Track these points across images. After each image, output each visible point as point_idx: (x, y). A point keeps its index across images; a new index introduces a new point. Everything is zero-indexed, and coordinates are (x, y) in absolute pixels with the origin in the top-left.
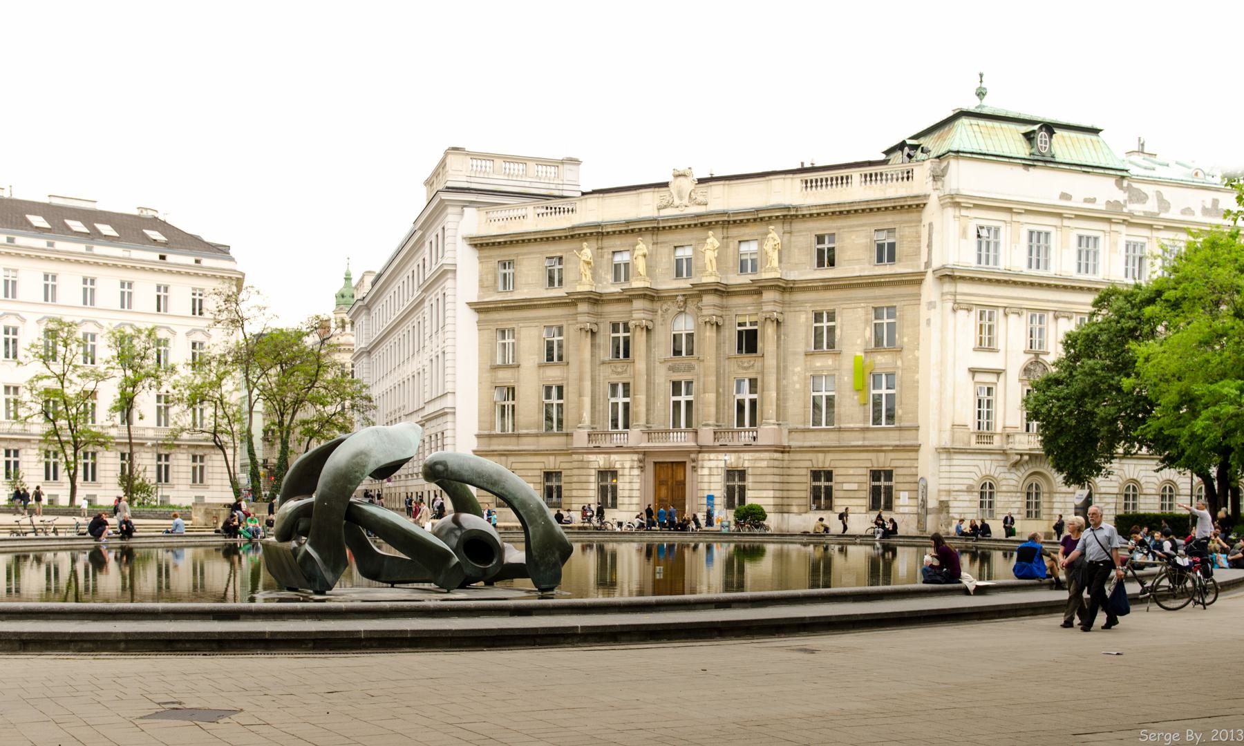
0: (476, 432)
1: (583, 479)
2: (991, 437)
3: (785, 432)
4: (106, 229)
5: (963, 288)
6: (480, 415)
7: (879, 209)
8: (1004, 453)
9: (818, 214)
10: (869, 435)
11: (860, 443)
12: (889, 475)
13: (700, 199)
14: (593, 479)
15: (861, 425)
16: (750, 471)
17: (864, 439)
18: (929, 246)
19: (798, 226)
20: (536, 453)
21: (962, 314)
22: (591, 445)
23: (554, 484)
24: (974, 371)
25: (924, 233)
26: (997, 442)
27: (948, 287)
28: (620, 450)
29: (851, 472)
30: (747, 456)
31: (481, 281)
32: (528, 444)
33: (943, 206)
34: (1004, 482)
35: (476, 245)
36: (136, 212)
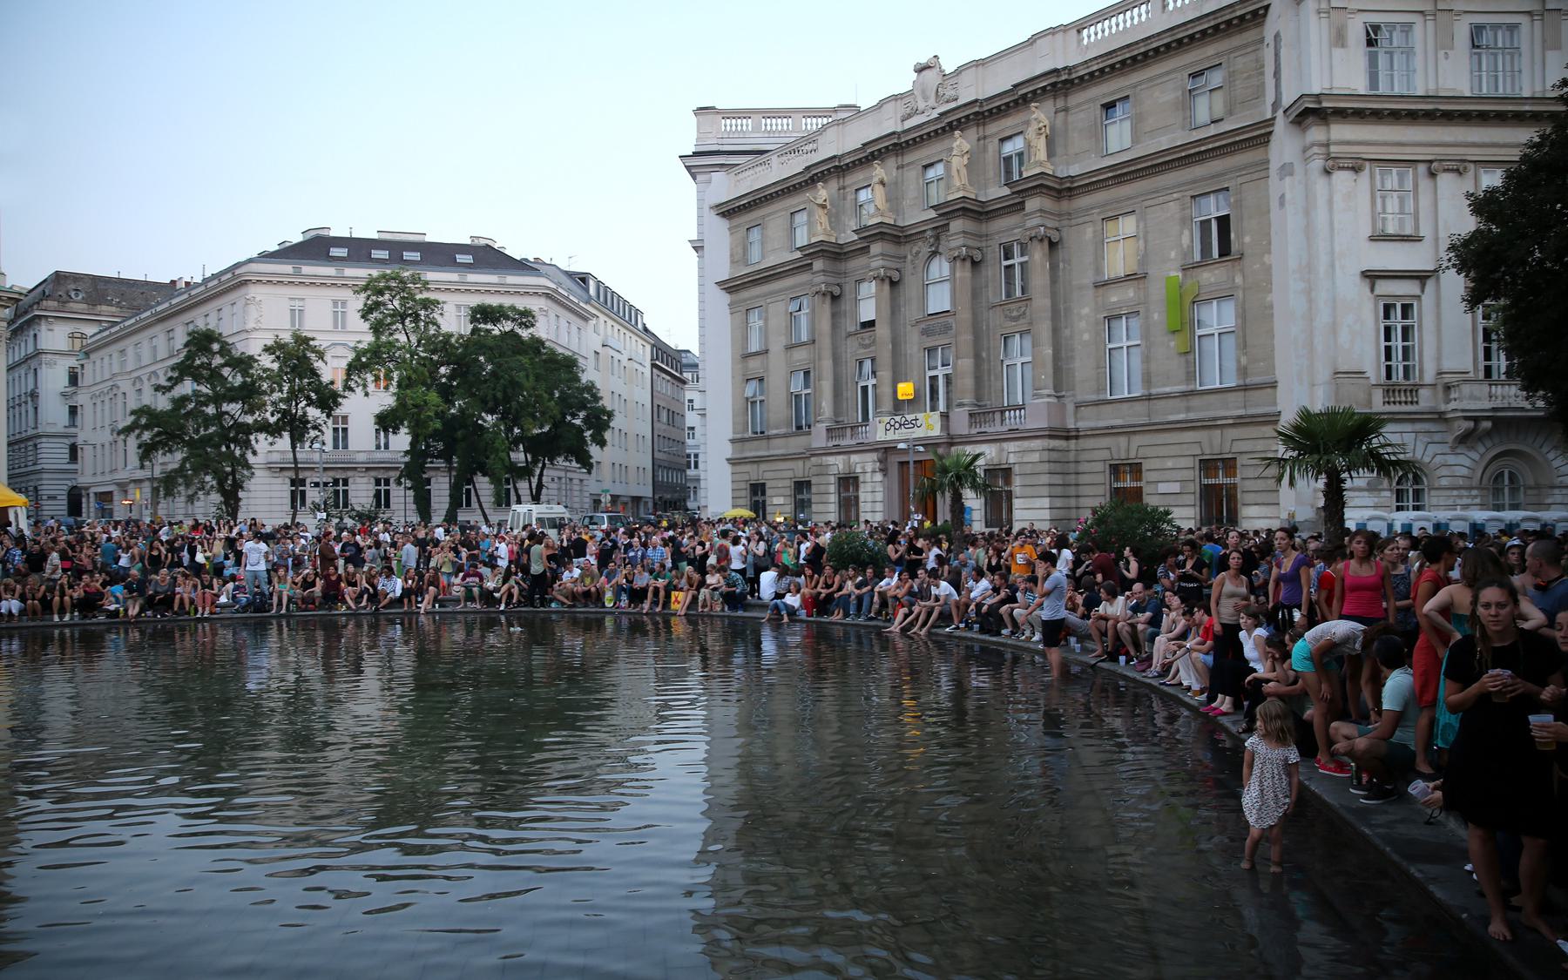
1: (822, 488)
2: (1414, 390)
3: (1070, 408)
4: (407, 255)
5: (1341, 131)
7: (1192, 37)
8: (1440, 417)
9: (1102, 70)
11: (1181, 417)
13: (950, 93)
14: (832, 489)
15: (1183, 388)
16: (1016, 469)
17: (1188, 410)
19: (1076, 99)
20: (784, 458)
21: (1342, 178)
24: (1372, 277)
26: (1426, 400)
27: (1316, 133)
28: (862, 449)
29: (1170, 464)
30: (1012, 446)
32: (778, 447)
34: (1444, 471)
35: (723, 215)
36: (468, 242)
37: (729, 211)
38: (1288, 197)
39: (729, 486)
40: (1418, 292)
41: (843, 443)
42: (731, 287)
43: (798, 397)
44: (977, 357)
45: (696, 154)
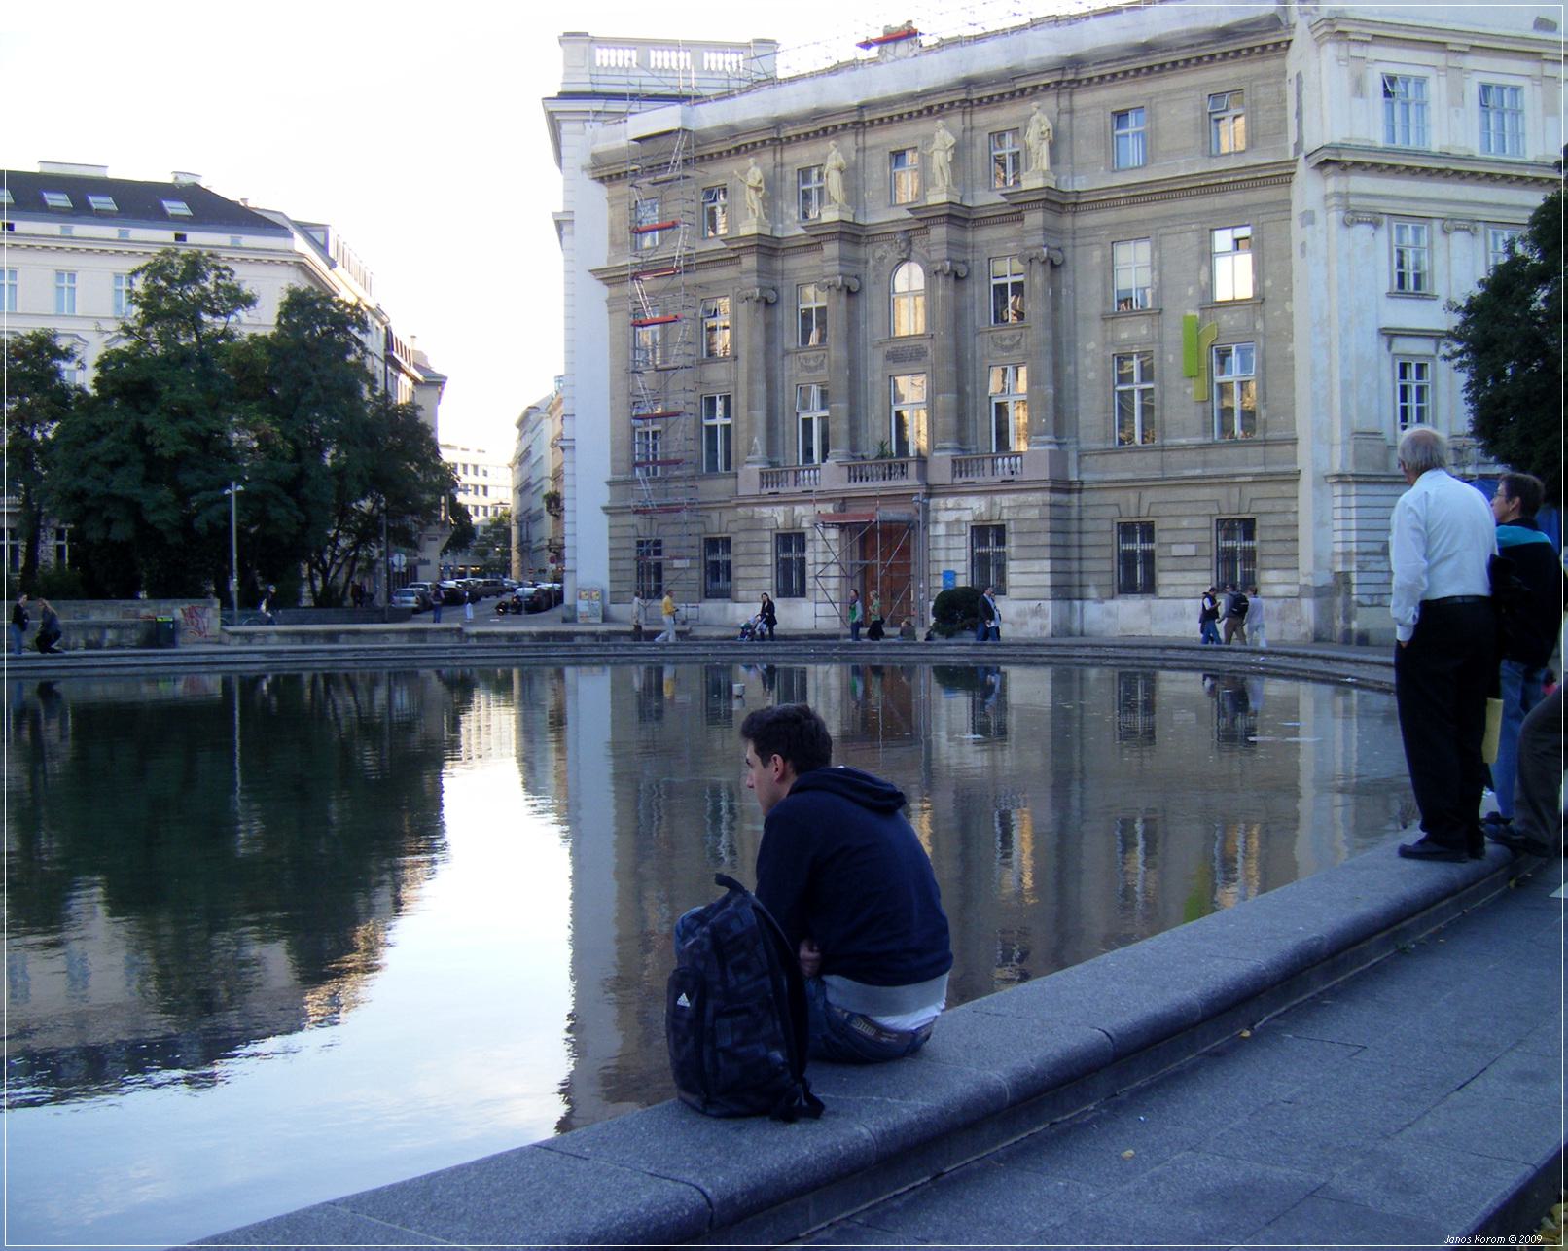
0: (608, 476)
1: (755, 548)
3: (1073, 456)
6: (614, 450)
10: (1213, 455)
11: (1198, 472)
12: (1248, 527)
14: (768, 548)
15: (1200, 440)
16: (1011, 527)
17: (1205, 464)
18: (1299, 114)
21: (1363, 230)
22: (765, 491)
23: (721, 557)
24: (1390, 334)
25: (1291, 91)
27: (1334, 183)
28: (807, 497)
29: (1185, 523)
30: (1005, 500)
31: (612, 235)
33: (1319, 42)
35: (602, 180)
37: (608, 172)
38: (1309, 245)
39: (606, 543)
40: (1431, 351)
41: (782, 490)
42: (610, 277)
43: (712, 430)
44: (960, 391)
45: (565, 96)
